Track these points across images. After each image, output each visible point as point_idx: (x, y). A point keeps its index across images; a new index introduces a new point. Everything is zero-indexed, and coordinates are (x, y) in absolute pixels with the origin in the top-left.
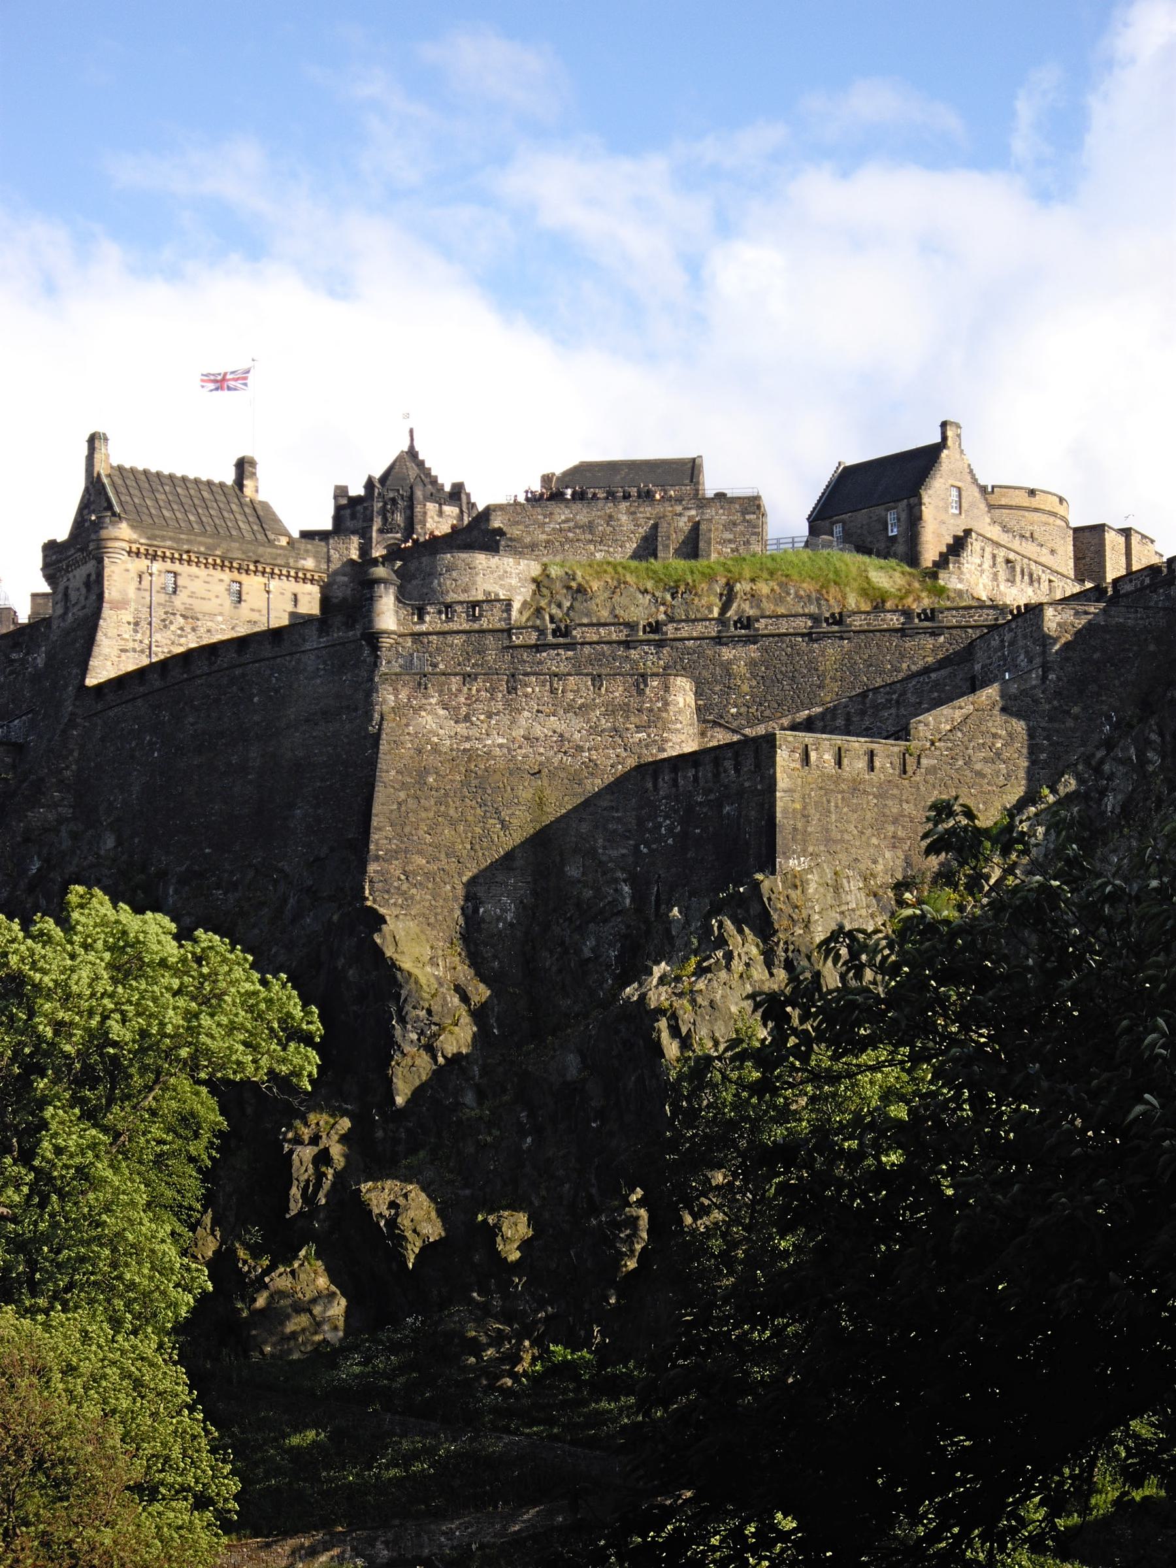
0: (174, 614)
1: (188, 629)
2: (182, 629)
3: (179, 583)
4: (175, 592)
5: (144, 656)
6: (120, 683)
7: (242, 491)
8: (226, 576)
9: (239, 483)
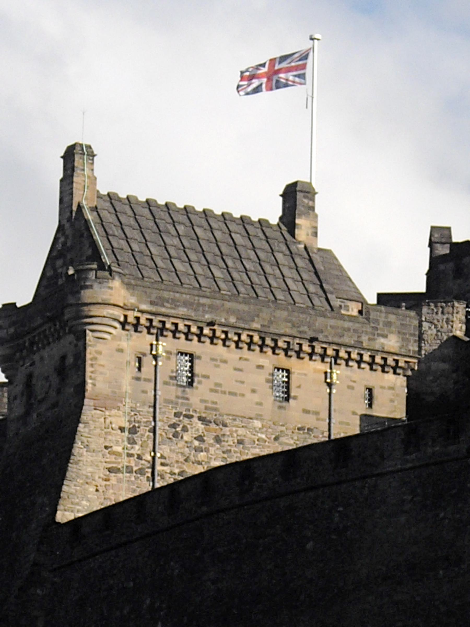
0: (189, 417)
1: (209, 439)
2: (200, 438)
3: (197, 370)
4: (191, 384)
5: (144, 479)
6: (107, 518)
7: (293, 235)
8: (268, 360)
9: (289, 219)
